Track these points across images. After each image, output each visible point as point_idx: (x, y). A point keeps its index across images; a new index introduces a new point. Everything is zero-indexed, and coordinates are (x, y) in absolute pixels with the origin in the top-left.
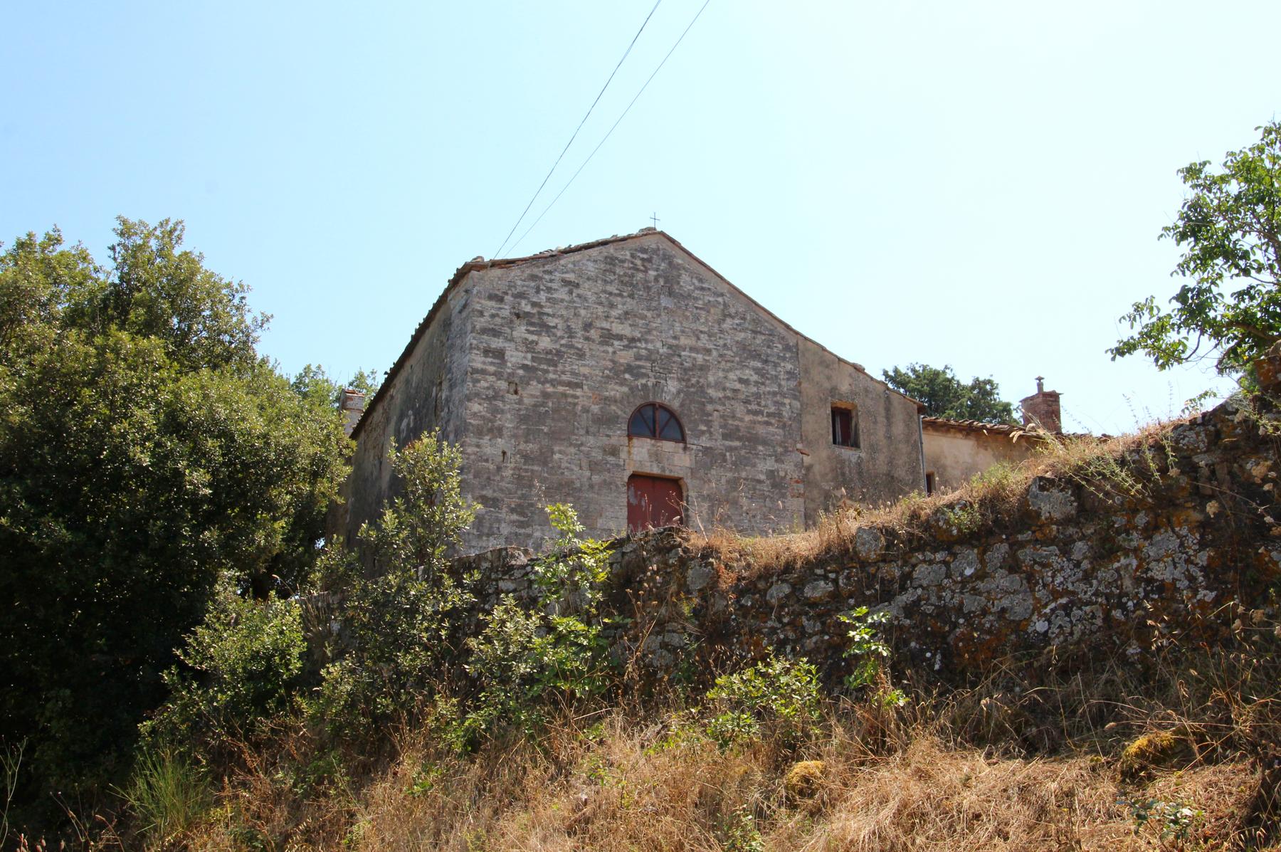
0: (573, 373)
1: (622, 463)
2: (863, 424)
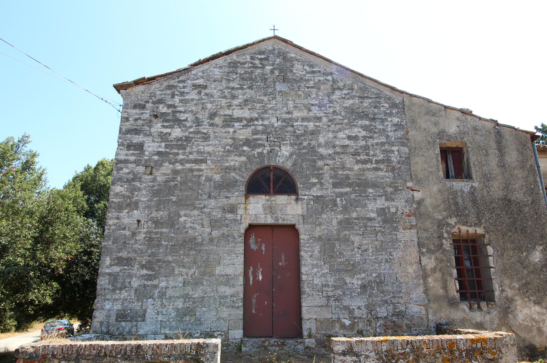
0: (199, 152)
1: (239, 218)
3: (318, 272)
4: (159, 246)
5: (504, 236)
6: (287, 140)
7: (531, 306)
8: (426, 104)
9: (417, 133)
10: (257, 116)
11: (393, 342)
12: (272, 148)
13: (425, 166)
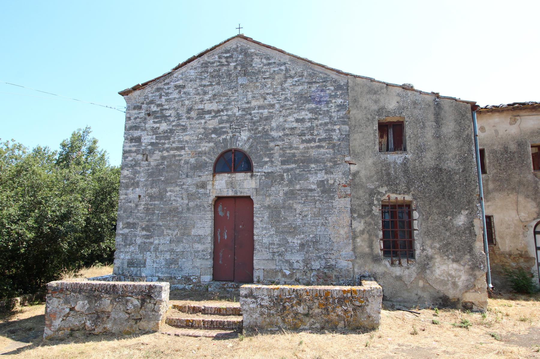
0: (180, 141)
1: (208, 192)
2: (408, 131)
3: (266, 233)
4: (153, 214)
5: (430, 202)
6: (246, 127)
7: (449, 263)
8: (369, 83)
9: (358, 112)
10: (222, 108)
11: (283, 290)
12: (234, 134)
13: (363, 141)
